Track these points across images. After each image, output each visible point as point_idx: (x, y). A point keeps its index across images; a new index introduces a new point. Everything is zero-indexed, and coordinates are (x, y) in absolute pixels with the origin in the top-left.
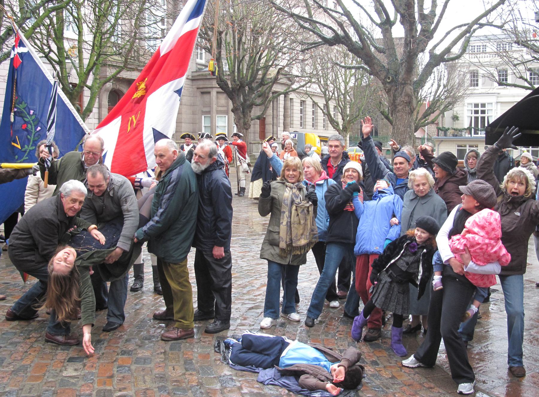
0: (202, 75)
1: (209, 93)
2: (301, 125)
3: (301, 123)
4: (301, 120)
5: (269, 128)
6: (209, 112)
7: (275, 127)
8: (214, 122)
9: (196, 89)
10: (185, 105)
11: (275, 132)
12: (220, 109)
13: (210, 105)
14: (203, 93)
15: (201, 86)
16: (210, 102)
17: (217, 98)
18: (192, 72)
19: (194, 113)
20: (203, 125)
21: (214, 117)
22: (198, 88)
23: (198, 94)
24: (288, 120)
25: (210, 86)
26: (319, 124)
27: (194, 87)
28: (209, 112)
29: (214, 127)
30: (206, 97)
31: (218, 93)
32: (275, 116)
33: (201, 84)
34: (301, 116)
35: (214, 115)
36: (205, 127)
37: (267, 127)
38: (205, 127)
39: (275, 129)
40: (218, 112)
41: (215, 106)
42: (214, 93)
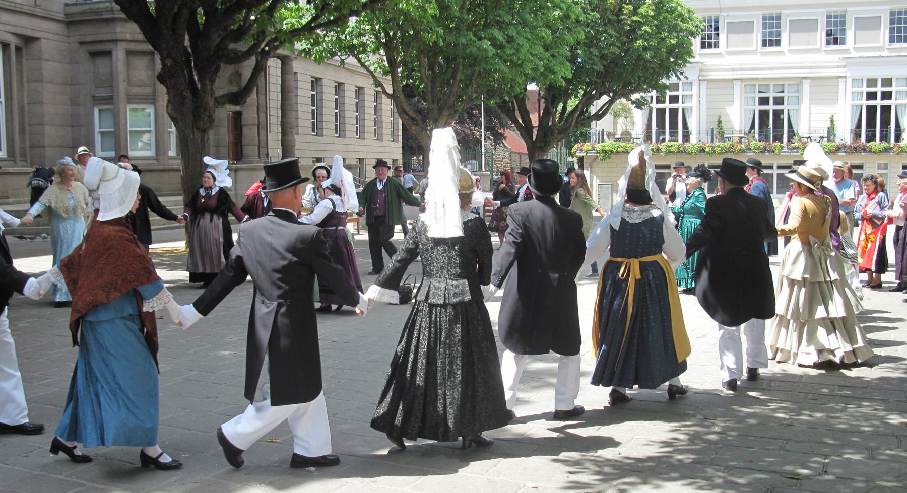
0: (91, 12)
1: (109, 53)
2: (313, 131)
3: (313, 123)
4: (313, 119)
5: (250, 133)
6: (110, 100)
7: (262, 132)
8: (122, 121)
9: (76, 46)
10: (51, 82)
11: (263, 144)
12: (135, 90)
13: (110, 82)
14: (94, 55)
15: (89, 39)
16: (111, 74)
17: (128, 65)
18: (66, 5)
19: (74, 102)
20: (97, 129)
21: (122, 110)
22: (81, 43)
23: (83, 56)
24: (291, 115)
25: (109, 37)
26: (347, 127)
27: (72, 39)
28: (110, 100)
29: (122, 133)
30: (102, 64)
31: (129, 53)
32: (262, 109)
33: (89, 33)
34: (313, 110)
35: (122, 105)
36: (102, 133)
37: (245, 131)
38: (102, 133)
39: (263, 138)
40: (131, 99)
41: (122, 86)
42: (119, 53)
